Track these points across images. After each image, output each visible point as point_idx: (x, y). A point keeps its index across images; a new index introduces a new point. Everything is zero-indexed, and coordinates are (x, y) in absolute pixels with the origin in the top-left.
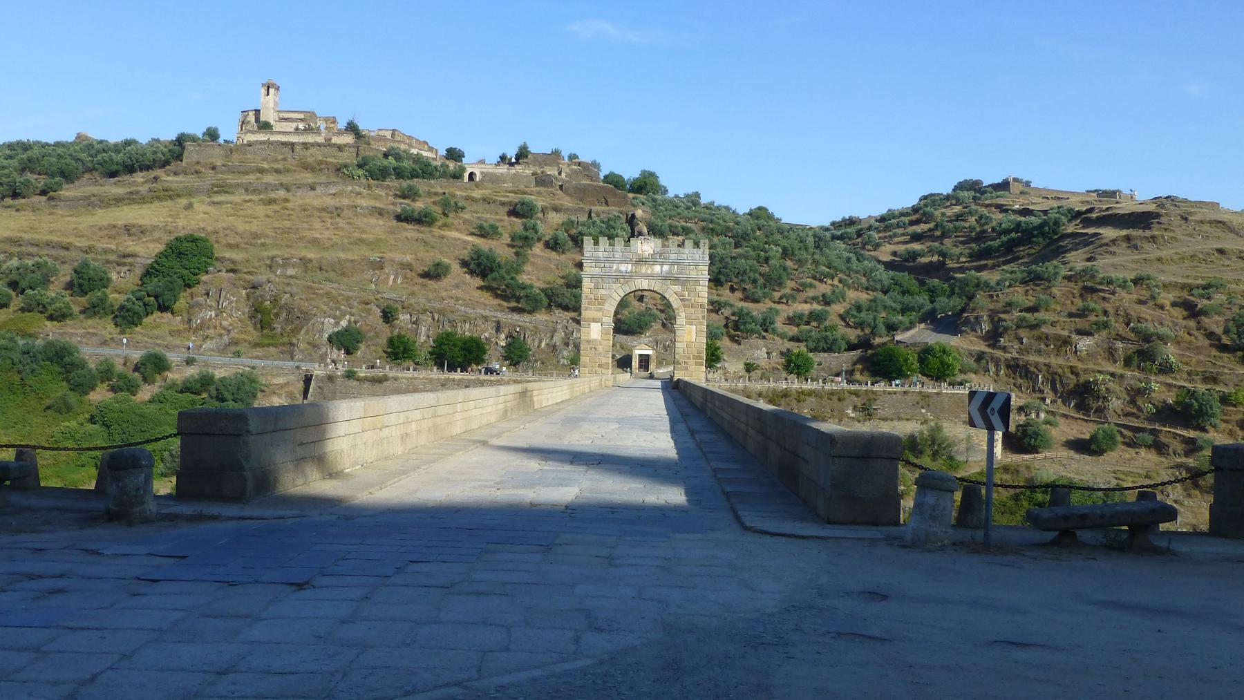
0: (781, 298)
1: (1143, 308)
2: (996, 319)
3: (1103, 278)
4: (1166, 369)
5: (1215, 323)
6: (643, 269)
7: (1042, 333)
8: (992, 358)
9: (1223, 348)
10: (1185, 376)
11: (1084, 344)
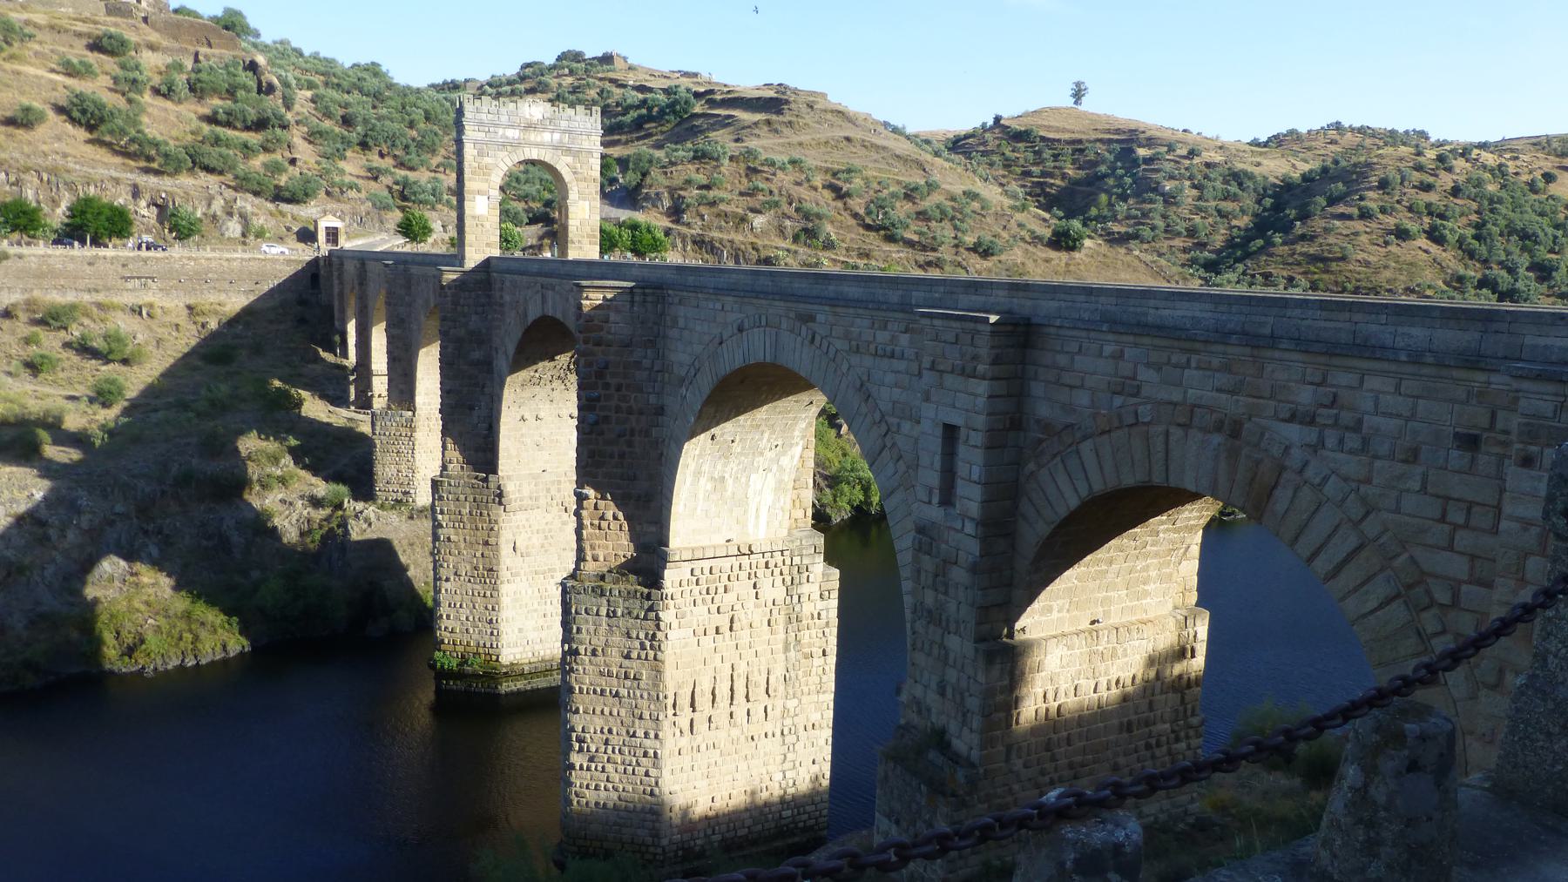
1: (801, 189)
2: (676, 196)
3: (766, 160)
4: (829, 245)
5: (858, 205)
6: (533, 136)
7: (721, 211)
8: (679, 234)
9: (868, 227)
10: (844, 252)
11: (759, 221)
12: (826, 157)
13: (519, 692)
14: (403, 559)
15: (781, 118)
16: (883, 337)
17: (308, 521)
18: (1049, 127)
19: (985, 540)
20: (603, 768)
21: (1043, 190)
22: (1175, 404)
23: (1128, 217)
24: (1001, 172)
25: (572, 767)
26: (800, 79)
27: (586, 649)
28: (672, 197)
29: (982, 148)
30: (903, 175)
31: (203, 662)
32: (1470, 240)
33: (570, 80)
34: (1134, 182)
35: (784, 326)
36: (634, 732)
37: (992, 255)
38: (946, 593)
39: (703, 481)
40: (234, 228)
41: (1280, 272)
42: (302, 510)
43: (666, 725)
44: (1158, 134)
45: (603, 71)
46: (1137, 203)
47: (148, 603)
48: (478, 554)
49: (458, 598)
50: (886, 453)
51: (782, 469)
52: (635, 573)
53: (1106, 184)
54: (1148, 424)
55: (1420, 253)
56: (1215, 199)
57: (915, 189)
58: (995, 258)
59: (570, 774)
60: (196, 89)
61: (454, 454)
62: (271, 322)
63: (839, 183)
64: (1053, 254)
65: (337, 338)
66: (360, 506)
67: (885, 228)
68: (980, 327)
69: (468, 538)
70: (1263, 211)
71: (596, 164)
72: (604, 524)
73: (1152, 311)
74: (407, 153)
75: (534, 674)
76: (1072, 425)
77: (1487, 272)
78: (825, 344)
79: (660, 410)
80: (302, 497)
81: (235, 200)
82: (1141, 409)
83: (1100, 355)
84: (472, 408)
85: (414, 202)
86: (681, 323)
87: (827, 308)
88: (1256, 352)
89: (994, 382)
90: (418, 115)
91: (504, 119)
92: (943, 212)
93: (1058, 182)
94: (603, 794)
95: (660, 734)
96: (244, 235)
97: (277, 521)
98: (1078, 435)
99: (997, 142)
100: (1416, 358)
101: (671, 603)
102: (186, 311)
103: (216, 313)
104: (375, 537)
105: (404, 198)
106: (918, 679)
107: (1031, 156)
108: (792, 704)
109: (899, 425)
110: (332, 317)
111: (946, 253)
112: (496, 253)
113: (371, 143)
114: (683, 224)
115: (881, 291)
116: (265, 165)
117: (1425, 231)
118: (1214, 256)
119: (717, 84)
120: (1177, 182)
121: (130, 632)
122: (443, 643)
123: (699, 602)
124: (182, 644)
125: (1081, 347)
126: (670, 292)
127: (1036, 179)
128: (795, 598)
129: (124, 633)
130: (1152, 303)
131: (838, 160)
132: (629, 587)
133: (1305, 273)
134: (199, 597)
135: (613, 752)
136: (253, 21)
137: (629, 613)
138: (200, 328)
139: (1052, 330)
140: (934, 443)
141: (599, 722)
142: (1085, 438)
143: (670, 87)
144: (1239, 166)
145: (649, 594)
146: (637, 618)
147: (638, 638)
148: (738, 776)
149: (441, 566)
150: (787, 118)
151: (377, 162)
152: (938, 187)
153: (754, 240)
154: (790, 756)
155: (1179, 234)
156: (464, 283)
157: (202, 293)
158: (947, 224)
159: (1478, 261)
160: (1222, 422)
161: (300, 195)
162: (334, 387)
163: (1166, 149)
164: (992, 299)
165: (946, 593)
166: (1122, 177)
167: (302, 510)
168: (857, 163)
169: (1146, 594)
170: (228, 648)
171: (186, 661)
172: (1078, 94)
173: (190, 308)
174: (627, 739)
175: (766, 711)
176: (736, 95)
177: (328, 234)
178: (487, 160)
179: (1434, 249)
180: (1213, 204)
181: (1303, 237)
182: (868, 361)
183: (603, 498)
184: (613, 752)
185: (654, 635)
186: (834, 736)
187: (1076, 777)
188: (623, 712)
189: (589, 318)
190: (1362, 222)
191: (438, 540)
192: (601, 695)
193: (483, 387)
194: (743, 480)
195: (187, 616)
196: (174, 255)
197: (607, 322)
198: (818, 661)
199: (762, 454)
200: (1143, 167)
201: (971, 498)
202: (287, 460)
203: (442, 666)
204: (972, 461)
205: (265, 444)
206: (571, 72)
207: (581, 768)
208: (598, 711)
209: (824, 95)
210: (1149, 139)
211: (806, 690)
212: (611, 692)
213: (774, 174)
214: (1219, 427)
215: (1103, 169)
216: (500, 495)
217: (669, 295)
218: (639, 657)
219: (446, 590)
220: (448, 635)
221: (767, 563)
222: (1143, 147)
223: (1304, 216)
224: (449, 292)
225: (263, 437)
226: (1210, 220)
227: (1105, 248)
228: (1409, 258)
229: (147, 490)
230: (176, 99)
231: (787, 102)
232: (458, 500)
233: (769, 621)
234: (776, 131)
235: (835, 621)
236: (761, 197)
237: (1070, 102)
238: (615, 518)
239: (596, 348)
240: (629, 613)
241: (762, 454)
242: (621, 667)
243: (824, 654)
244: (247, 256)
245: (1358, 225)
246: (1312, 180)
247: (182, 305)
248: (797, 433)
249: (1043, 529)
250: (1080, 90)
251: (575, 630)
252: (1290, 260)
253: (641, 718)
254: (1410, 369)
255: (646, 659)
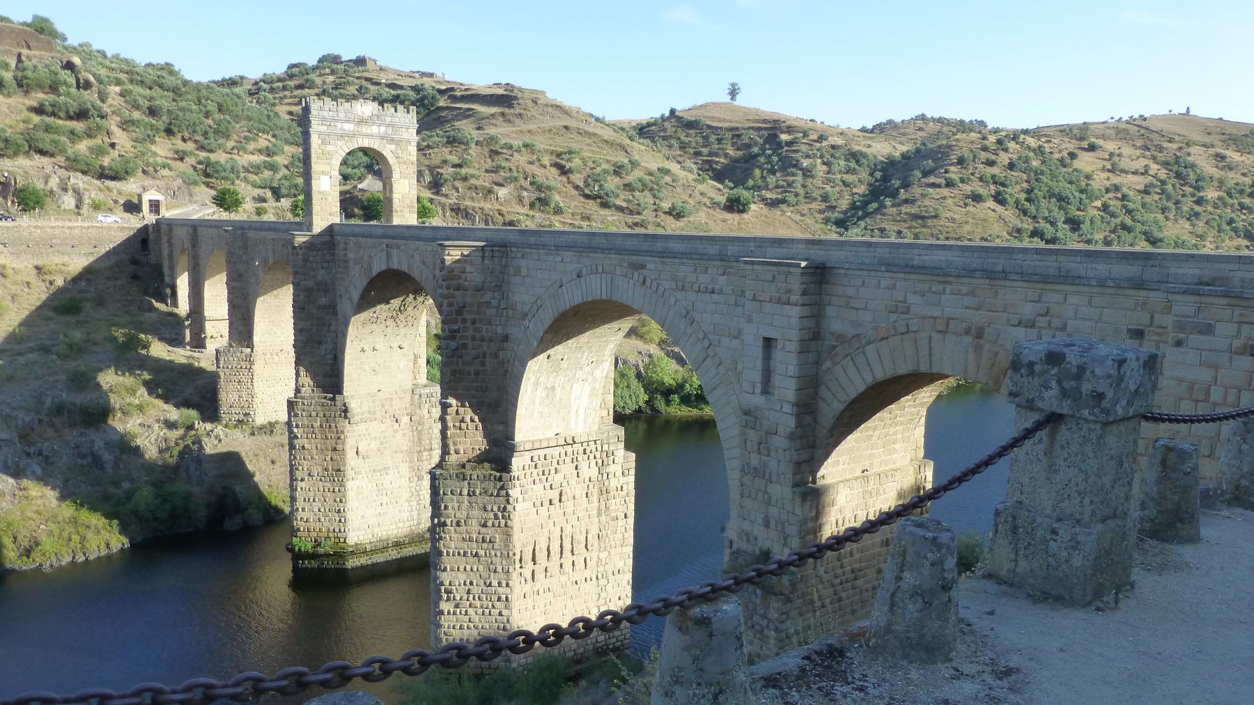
0: (232, 149)
1: (530, 166)
2: (435, 173)
3: (505, 144)
4: (558, 211)
5: (578, 179)
7: (472, 184)
8: (440, 203)
9: (587, 197)
10: (570, 216)
11: (502, 192)
12: (551, 142)
13: (362, 567)
14: (250, 467)
15: (512, 111)
16: (704, 279)
17: (166, 440)
18: (713, 117)
19: (799, 416)
20: (466, 612)
21: (711, 166)
22: (935, 318)
23: (777, 187)
24: (679, 153)
25: (442, 613)
26: (523, 79)
27: (452, 522)
28: (432, 174)
29: (662, 134)
30: (611, 155)
31: (91, 558)
32: (1023, 202)
33: (331, 78)
34: (780, 160)
35: (618, 272)
36: (490, 583)
37: (683, 217)
38: (768, 455)
39: (539, 389)
40: (69, 201)
41: (891, 227)
42: (159, 431)
43: (515, 575)
44: (795, 123)
45: (359, 72)
46: (783, 176)
47: (37, 512)
48: (328, 458)
49: (311, 494)
50: (709, 361)
51: (595, 380)
52: (489, 461)
53: (758, 161)
54: (916, 332)
55: (990, 211)
56: (840, 172)
57: (621, 167)
58: (685, 219)
59: (440, 618)
60: (23, 85)
61: (306, 380)
62: (109, 279)
63: (563, 162)
64: (728, 216)
65: (168, 291)
66: (209, 426)
67: (600, 197)
68: (792, 270)
69: (319, 445)
70: (875, 181)
71: (413, 149)
72: (464, 425)
73: (917, 257)
74: (206, 138)
75: (398, 544)
76: (858, 335)
77: (1037, 225)
78: (655, 284)
79: (506, 338)
80: (158, 421)
81: (69, 178)
82: (910, 322)
83: (879, 287)
84: (320, 343)
85: (217, 178)
86: (524, 272)
87: (657, 259)
88: (992, 282)
89: (802, 307)
90: (212, 107)
91: (342, 115)
92: (644, 185)
93: (722, 160)
94: (466, 632)
95: (510, 583)
96: (77, 207)
97: (139, 442)
98: (864, 342)
99: (674, 129)
100: (1102, 284)
101: (517, 483)
102: (35, 272)
103: (61, 272)
104: (225, 450)
105: (207, 175)
106: (746, 517)
107: (700, 140)
108: (603, 555)
109: (719, 340)
110: (161, 275)
111: (648, 215)
112: (337, 220)
113: (175, 130)
114: (442, 195)
115: (702, 246)
116: (91, 149)
117: (992, 196)
118: (842, 216)
119: (454, 83)
120: (812, 160)
121: (25, 537)
122: (299, 530)
123: (537, 481)
124: (72, 544)
125: (864, 282)
126: (513, 249)
127: (705, 158)
128: (605, 475)
129: (20, 538)
130: (916, 251)
131: (560, 144)
132: (484, 472)
133: (909, 228)
134: (82, 505)
135: (474, 599)
136: (59, 26)
137: (486, 492)
138: (48, 285)
139: (842, 271)
140: (757, 350)
141: (462, 577)
142: (869, 343)
143: (417, 86)
144: (856, 148)
145: (501, 477)
146: (492, 495)
147: (492, 510)
148: (566, 612)
149: (297, 469)
150: (517, 111)
151: (181, 146)
152: (639, 164)
153: (500, 207)
154: (603, 595)
155: (815, 199)
156: (310, 246)
157: (48, 256)
158: (647, 193)
159: (1029, 217)
160: (970, 328)
161: (122, 173)
162: (171, 330)
163: (801, 135)
164: (793, 251)
165: (768, 455)
166: (770, 156)
167: (159, 431)
168: (575, 146)
169: (895, 450)
170: (111, 546)
171: (77, 557)
172: (733, 93)
173: (38, 268)
174: (485, 588)
175: (585, 562)
176: (473, 92)
177: (151, 206)
178: (329, 148)
179: (999, 208)
180: (839, 176)
181: (906, 201)
182: (691, 296)
183: (463, 406)
184: (474, 599)
185: (505, 508)
186: (634, 578)
187: (856, 579)
188: (481, 568)
189: (451, 270)
190: (947, 189)
191: (295, 448)
192: (464, 556)
193: (329, 327)
194: (568, 388)
195: (74, 521)
196: (22, 224)
197: (464, 272)
198: (621, 522)
199: (581, 369)
200: (786, 148)
201: (787, 388)
202: (142, 391)
203: (300, 550)
204: (787, 363)
205: (121, 379)
206: (333, 72)
207: (449, 613)
208: (462, 568)
209: (543, 93)
210: (789, 127)
211: (613, 544)
212: (471, 553)
213: (512, 156)
214: (967, 332)
215: (756, 150)
216: (346, 411)
217: (512, 252)
218: (493, 525)
219: (302, 488)
220: (304, 524)
221: (585, 450)
222: (785, 133)
223: (906, 185)
224: (300, 252)
225: (119, 373)
226: (837, 188)
227: (765, 210)
228: (982, 216)
229: (27, 419)
230: (6, 93)
231: (516, 98)
232: (310, 416)
233: (587, 494)
234: (510, 121)
235: (633, 492)
236: (503, 174)
237: (727, 99)
238: (472, 421)
239: (456, 292)
240: (486, 492)
241: (582, 369)
242: (479, 533)
243: (626, 517)
244: (86, 224)
245: (945, 192)
246: (909, 158)
247: (31, 266)
248: (607, 352)
249: (837, 407)
250: (735, 90)
251: (443, 508)
252: (899, 218)
253: (495, 571)
254: (1097, 290)
255: (499, 526)
